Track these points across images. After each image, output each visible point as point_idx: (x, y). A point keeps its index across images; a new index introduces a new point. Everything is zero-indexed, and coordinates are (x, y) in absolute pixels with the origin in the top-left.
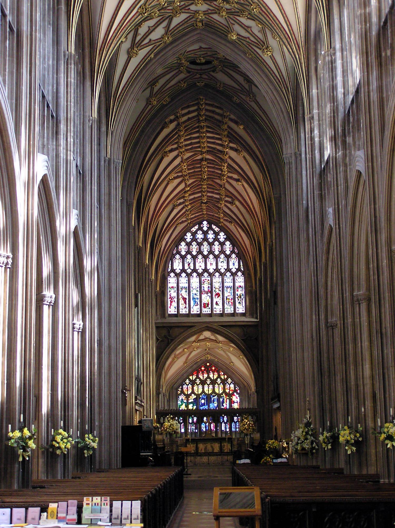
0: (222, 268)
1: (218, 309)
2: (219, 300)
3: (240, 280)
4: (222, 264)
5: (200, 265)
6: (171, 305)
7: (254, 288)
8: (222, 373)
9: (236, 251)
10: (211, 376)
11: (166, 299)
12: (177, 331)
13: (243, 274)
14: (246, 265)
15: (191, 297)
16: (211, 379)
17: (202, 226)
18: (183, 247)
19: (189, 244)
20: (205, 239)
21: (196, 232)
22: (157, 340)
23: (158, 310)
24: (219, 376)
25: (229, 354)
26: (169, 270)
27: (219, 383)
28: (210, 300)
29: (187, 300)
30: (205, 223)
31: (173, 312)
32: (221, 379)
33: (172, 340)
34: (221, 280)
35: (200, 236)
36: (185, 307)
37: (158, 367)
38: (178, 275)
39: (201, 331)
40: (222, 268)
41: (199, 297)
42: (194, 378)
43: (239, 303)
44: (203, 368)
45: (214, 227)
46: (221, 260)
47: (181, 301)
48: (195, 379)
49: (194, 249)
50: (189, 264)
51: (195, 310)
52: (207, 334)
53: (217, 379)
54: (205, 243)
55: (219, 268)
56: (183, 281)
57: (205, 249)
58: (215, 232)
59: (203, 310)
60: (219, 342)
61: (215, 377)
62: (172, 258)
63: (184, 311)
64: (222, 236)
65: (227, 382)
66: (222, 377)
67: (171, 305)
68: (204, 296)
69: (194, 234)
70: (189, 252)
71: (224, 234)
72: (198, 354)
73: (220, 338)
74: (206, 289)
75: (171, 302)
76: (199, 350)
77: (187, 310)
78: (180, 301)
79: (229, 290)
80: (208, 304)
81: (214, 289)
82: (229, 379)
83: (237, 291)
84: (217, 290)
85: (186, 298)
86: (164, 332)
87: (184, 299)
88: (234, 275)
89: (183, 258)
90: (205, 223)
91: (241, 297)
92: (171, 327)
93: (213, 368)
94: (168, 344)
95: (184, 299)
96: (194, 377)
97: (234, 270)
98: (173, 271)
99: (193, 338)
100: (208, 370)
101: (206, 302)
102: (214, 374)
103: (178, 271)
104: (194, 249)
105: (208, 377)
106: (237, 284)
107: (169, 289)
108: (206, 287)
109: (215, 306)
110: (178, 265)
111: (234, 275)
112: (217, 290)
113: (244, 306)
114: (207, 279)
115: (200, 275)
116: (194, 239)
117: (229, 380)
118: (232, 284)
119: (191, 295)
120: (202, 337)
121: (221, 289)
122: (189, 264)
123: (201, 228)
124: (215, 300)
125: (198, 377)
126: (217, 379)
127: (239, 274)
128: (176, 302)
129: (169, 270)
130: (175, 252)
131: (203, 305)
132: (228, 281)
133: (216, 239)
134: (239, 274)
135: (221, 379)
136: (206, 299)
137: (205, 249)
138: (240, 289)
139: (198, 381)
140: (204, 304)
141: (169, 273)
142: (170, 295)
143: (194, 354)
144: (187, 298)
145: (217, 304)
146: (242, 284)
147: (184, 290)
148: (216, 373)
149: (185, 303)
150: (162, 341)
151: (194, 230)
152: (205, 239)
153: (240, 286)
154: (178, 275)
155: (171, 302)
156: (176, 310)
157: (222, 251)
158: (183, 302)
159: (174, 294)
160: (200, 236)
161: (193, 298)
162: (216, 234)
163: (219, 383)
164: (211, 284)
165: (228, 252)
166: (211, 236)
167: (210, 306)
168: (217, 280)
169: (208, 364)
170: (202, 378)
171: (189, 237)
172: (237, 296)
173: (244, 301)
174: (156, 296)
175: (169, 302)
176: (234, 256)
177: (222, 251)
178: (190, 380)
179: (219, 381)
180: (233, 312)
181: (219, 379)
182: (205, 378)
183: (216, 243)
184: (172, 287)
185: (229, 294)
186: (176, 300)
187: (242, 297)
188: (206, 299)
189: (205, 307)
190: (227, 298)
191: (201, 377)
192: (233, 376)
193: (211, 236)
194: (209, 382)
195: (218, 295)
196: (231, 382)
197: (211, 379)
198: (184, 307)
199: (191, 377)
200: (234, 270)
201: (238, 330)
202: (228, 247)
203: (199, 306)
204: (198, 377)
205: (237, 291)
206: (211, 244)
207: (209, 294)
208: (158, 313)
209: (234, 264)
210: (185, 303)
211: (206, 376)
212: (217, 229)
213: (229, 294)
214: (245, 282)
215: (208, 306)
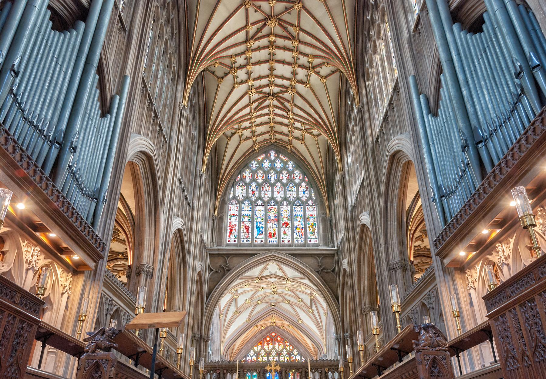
0: (291, 197)
1: (286, 239)
2: (288, 230)
3: (312, 210)
4: (291, 193)
5: (266, 193)
6: (230, 234)
7: (328, 215)
8: (288, 344)
9: (306, 179)
10: (276, 347)
11: (224, 225)
12: (235, 260)
13: (315, 202)
14: (318, 193)
15: (255, 226)
16: (276, 351)
17: (269, 155)
18: (247, 174)
19: (254, 172)
20: (273, 168)
21: (262, 161)
22: (211, 270)
23: (214, 236)
24: (285, 348)
25: (298, 309)
26: (231, 197)
27: (284, 355)
28: (277, 229)
29: (250, 229)
30: (272, 152)
31: (232, 242)
32: (287, 350)
33: (228, 271)
34: (289, 209)
35: (266, 165)
36: (248, 236)
37: (209, 303)
38: (240, 203)
39: (265, 261)
40: (291, 197)
41: (263, 226)
42: (259, 349)
43: (311, 233)
44: (268, 339)
45: (282, 156)
46: (290, 189)
47: (243, 230)
48: (260, 351)
49: (260, 176)
50: (253, 192)
51: (260, 239)
52: (273, 267)
53: (282, 350)
54: (272, 172)
55: (288, 196)
56: (246, 209)
57: (272, 178)
58: (282, 161)
59: (268, 240)
60: (289, 279)
61: (281, 347)
62: (234, 184)
63: (245, 239)
64: (291, 165)
65: (293, 354)
66: (288, 348)
67: (230, 234)
68: (269, 225)
69: (260, 163)
70: (254, 180)
71: (292, 163)
72: (263, 309)
73: (290, 272)
74: (273, 218)
75: (231, 231)
76: (263, 306)
77: (250, 240)
78: (242, 229)
79: (299, 219)
80: (274, 234)
81: (281, 218)
82: (295, 350)
83: (309, 220)
84: (285, 219)
85: (248, 227)
86: (220, 262)
87: (247, 228)
88: (304, 204)
89: (247, 185)
90: (272, 152)
91: (313, 227)
92: (228, 255)
93: (279, 339)
94: (224, 275)
95: (247, 228)
96: (259, 348)
97: (304, 199)
98: (235, 197)
99: (256, 271)
100: (273, 340)
101: (272, 231)
102: (279, 345)
103: (241, 198)
104: (260, 176)
105: (274, 348)
106: (308, 213)
107: (229, 217)
108: (272, 215)
109: (282, 236)
110: (240, 192)
111: (304, 204)
112: (285, 219)
113: (317, 236)
114: (274, 207)
115: (265, 203)
116: (260, 167)
117: (295, 351)
118: (302, 213)
119: (255, 223)
120: (266, 273)
121: (290, 218)
122: (253, 192)
123: (267, 157)
124: (282, 230)
125: (262, 348)
126: (282, 350)
127: (310, 203)
128: (237, 230)
129: (231, 197)
130: (238, 179)
131: (268, 235)
132: (298, 210)
133: (284, 168)
134: (310, 203)
135: (287, 350)
136: (272, 227)
137: (272, 178)
138: (311, 218)
139: (263, 353)
140: (270, 233)
141: (230, 200)
142: (230, 223)
143: (259, 308)
144: (250, 226)
145: (285, 233)
146: (314, 213)
147: (246, 219)
148: (281, 344)
149: (248, 231)
150: (217, 272)
151: (260, 158)
152: (273, 168)
153: (312, 215)
154: (240, 203)
155: (231, 231)
156: (236, 240)
157: (291, 180)
158: (245, 231)
159: (234, 222)
160: (266, 165)
161: (257, 227)
162: (285, 163)
163: (284, 355)
164: (279, 212)
165: (297, 181)
166: (278, 165)
167: (277, 235)
168: (285, 210)
169: (273, 334)
170: (267, 349)
171: (254, 165)
172: (308, 226)
173: (316, 231)
174: (213, 220)
175: (229, 231)
176: (304, 185)
177: (291, 180)
178: (254, 351)
179: (284, 352)
180: (304, 242)
181: (284, 350)
182: (270, 349)
183: (285, 172)
184: (233, 215)
185: (299, 223)
186: (237, 228)
187: (314, 226)
188: (272, 227)
189: (270, 237)
190: (296, 228)
191: (266, 347)
192: (299, 346)
193: (278, 165)
194: (274, 353)
195: (286, 224)
196: (297, 354)
197: (276, 351)
198: (246, 236)
199: (255, 348)
200: (304, 199)
201: (311, 261)
202: (297, 176)
203: (263, 236)
204: (262, 348)
205: (309, 220)
206: (278, 173)
207: (276, 223)
208: (214, 240)
209: (305, 192)
210: (248, 231)
211: (271, 346)
212: (285, 159)
213: (299, 223)
214: (318, 211)
215: (274, 236)
